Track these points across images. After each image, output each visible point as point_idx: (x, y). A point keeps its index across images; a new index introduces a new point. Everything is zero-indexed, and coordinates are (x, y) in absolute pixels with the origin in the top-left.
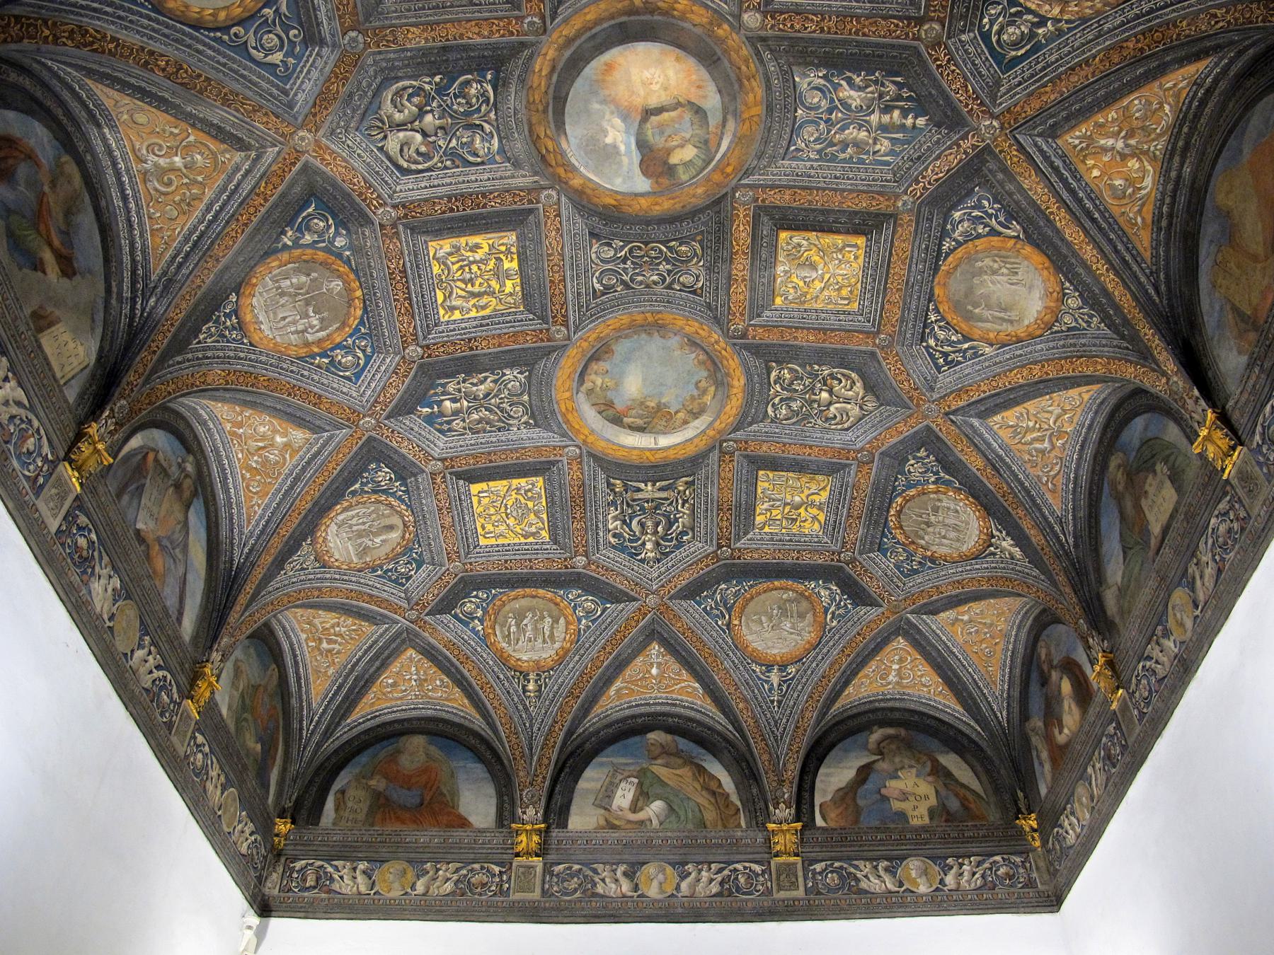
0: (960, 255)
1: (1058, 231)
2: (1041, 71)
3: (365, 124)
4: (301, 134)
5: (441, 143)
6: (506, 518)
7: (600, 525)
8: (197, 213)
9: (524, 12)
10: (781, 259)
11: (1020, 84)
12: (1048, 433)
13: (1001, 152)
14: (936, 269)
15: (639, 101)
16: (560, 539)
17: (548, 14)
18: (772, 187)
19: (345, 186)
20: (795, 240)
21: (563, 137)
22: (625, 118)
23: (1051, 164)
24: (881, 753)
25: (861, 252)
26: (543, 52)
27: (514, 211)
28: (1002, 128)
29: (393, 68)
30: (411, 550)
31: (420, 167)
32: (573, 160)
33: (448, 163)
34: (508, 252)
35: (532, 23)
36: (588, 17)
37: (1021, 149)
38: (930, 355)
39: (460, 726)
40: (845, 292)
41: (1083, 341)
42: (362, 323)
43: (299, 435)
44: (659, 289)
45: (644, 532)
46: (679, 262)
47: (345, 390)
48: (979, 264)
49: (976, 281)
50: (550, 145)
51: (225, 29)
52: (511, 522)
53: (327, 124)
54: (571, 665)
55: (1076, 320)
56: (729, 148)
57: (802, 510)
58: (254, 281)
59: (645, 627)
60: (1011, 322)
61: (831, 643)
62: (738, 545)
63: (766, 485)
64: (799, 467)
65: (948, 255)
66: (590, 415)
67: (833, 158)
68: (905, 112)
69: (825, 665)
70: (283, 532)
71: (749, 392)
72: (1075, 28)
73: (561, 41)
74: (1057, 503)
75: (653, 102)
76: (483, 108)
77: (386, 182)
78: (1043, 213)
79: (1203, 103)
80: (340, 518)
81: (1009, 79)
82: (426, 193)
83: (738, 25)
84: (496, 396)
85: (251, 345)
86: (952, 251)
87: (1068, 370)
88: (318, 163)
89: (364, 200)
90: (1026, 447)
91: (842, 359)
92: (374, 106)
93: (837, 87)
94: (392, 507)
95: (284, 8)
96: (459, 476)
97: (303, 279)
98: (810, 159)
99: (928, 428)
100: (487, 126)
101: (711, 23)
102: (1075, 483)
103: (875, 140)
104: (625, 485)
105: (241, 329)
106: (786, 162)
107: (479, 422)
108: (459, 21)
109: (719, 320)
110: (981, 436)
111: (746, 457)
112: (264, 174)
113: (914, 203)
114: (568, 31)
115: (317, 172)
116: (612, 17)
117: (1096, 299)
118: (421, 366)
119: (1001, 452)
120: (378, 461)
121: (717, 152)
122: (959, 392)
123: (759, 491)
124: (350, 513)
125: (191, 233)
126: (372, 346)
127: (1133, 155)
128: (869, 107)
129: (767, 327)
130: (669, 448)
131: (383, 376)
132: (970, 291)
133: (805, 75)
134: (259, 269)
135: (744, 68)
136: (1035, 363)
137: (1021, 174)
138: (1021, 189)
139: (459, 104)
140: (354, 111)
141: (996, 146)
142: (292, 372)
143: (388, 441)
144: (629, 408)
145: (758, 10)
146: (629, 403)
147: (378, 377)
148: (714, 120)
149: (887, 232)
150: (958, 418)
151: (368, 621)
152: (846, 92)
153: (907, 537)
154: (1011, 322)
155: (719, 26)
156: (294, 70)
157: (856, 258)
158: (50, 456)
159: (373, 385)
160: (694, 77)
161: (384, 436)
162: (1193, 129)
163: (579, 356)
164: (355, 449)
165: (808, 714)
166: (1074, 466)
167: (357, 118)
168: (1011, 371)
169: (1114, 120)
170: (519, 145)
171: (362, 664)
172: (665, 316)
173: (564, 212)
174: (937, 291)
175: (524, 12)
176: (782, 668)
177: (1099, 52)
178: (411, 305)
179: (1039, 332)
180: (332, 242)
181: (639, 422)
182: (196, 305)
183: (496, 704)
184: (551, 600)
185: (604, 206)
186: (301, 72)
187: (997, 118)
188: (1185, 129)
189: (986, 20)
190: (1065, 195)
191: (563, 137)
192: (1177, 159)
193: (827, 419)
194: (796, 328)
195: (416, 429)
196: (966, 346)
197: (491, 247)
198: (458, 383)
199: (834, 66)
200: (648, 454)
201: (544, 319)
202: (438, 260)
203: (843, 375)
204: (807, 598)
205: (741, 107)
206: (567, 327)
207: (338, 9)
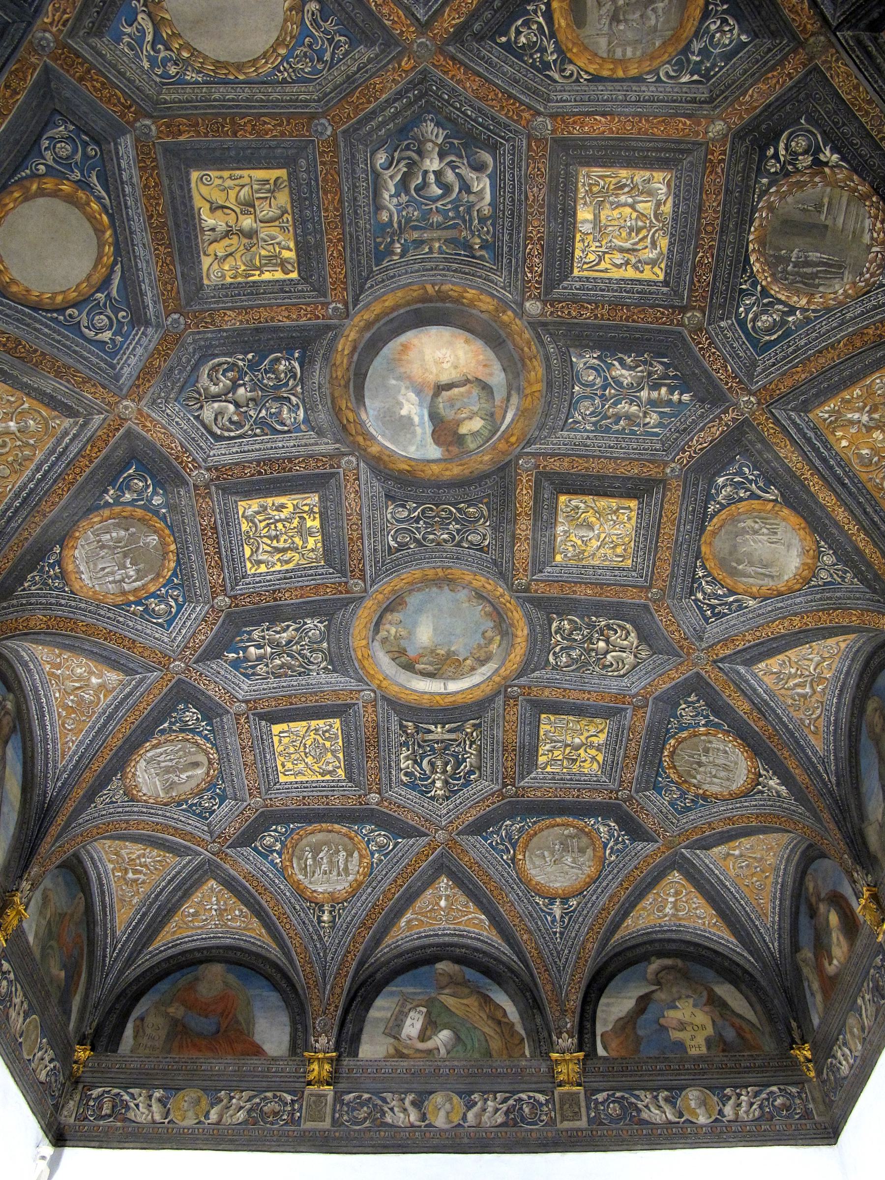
0: (724, 517)
1: (812, 495)
2: (792, 353)
3: (183, 395)
4: (125, 403)
5: (252, 413)
6: (305, 757)
7: (393, 764)
8: (28, 473)
9: (329, 299)
11: (774, 364)
12: (809, 679)
13: (758, 424)
14: (703, 529)
15: (431, 378)
16: (355, 776)
17: (350, 300)
18: (552, 455)
19: (164, 450)
20: (574, 503)
21: (363, 409)
22: (419, 392)
23: (804, 436)
24: (659, 983)
26: (346, 333)
27: (317, 475)
29: (208, 347)
30: (216, 785)
31: (232, 434)
32: (372, 430)
34: (311, 511)
35: (336, 309)
36: (387, 304)
37: (777, 422)
38: (699, 607)
39: (258, 956)
40: (619, 550)
42: (175, 574)
43: (113, 677)
44: (448, 546)
45: (433, 772)
46: (468, 523)
47: (157, 635)
48: (742, 525)
49: (739, 539)
50: (351, 416)
51: (61, 310)
52: (309, 760)
53: (149, 395)
54: (364, 898)
55: (831, 576)
56: (513, 420)
57: (581, 751)
58: (77, 534)
59: (434, 861)
60: (772, 577)
61: (610, 877)
62: (522, 784)
63: (548, 727)
64: (580, 711)
65: (713, 516)
66: (384, 660)
67: (608, 430)
69: (605, 899)
70: (94, 767)
71: (532, 639)
72: (821, 316)
73: (362, 324)
74: (818, 743)
75: (445, 378)
76: (290, 383)
77: (201, 447)
80: (149, 754)
81: (764, 360)
83: (521, 312)
84: (297, 643)
87: (826, 621)
88: (139, 429)
89: (181, 463)
90: (789, 693)
91: (617, 611)
92: (193, 379)
94: (198, 745)
95: (114, 293)
96: (262, 717)
97: (122, 533)
98: (586, 431)
99: (698, 674)
100: (293, 399)
101: (497, 310)
104: (416, 727)
105: (63, 578)
108: (271, 306)
109: (503, 575)
110: (747, 681)
111: (528, 701)
112: (91, 437)
113: (681, 470)
114: (368, 316)
115: (139, 437)
116: (408, 304)
117: (849, 557)
118: (229, 615)
119: (766, 697)
120: (186, 703)
121: (502, 423)
122: (726, 641)
123: (542, 733)
124: (158, 751)
125: (22, 489)
126: (184, 596)
127: (877, 428)
128: (639, 385)
129: (549, 582)
130: (457, 692)
131: (193, 623)
132: (734, 548)
133: (581, 356)
135: (526, 349)
136: (795, 614)
138: (777, 457)
139: (269, 379)
140: (174, 383)
141: (754, 419)
142: (108, 618)
143: (196, 683)
144: (421, 656)
145: (538, 298)
146: (421, 651)
148: (499, 396)
150: (726, 666)
151: (172, 852)
152: (618, 371)
153: (680, 777)
154: (772, 577)
155: (504, 312)
156: (121, 348)
157: (629, 519)
159: (184, 631)
160: (481, 357)
161: (193, 678)
164: (165, 690)
165: (589, 946)
166: (834, 709)
168: (773, 622)
169: (859, 397)
170: (322, 416)
171: (165, 894)
173: (363, 478)
174: (704, 549)
175: (329, 299)
176: (565, 900)
177: (843, 337)
178: (220, 558)
179: (798, 586)
180: (150, 501)
181: (430, 668)
182: (23, 556)
183: (292, 934)
184: (345, 835)
186: (127, 348)
187: (754, 394)
189: (741, 309)
190: (817, 463)
191: (363, 409)
193: (604, 667)
195: (222, 672)
196: (731, 599)
197: (296, 507)
198: (263, 631)
199: (607, 349)
200: (438, 698)
202: (246, 518)
203: (619, 626)
204: (587, 834)
205: (523, 384)
206: (364, 581)
207: (163, 295)
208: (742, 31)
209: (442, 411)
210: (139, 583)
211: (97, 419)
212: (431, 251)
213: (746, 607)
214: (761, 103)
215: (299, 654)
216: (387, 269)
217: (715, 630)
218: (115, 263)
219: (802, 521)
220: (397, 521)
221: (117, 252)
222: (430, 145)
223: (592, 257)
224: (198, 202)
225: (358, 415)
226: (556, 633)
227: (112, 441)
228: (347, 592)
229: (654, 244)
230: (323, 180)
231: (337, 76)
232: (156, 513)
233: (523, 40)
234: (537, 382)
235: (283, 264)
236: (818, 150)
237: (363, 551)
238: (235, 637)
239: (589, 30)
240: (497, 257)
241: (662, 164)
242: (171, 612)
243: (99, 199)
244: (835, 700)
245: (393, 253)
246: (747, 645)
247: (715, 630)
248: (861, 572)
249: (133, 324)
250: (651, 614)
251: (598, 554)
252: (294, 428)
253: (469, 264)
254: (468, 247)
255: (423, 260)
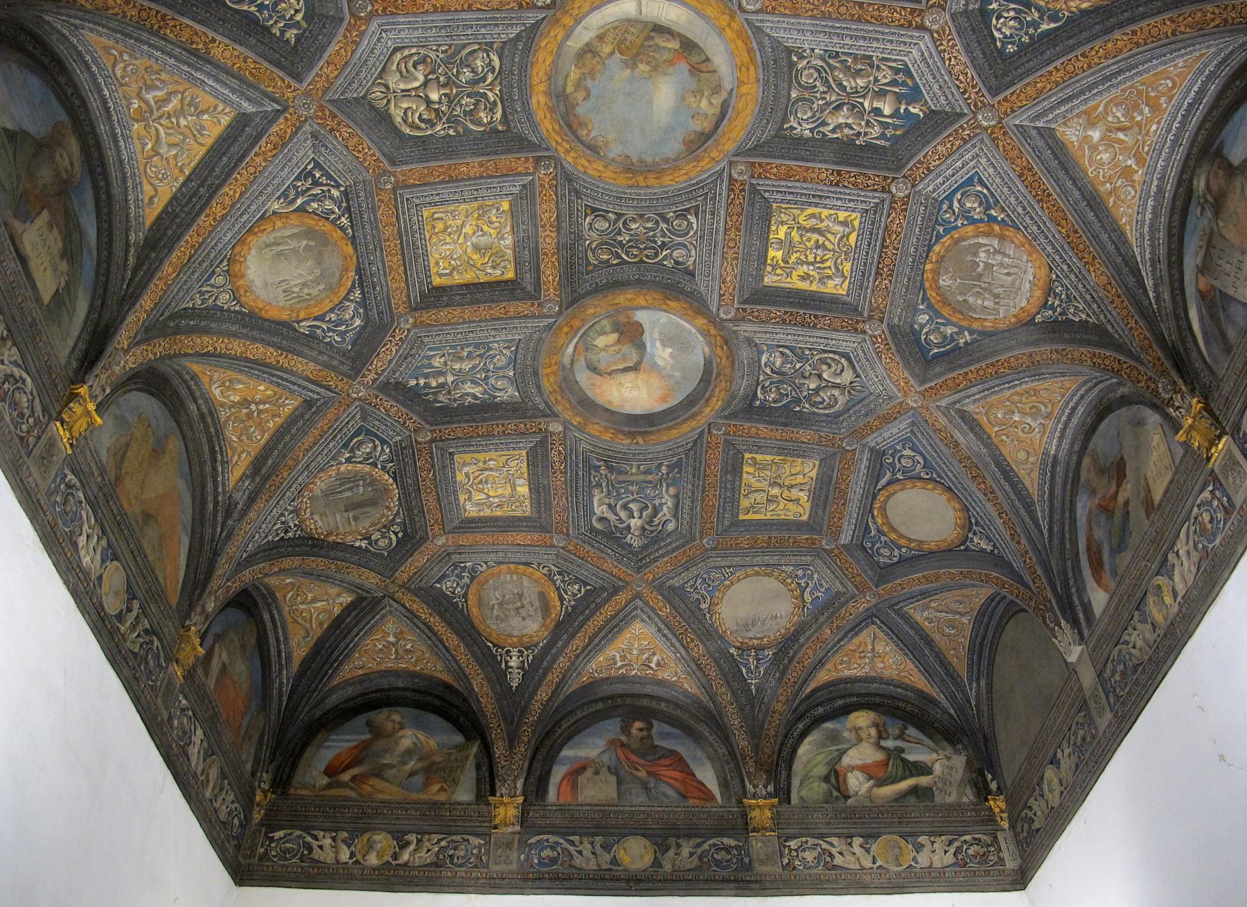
3: (863, 395)
8: (1024, 386)
10: (510, 252)
12: (156, 114)
14: (359, 270)
15: (642, 376)
18: (526, 316)
20: (498, 272)
22: (654, 367)
25: (434, 270)
28: (348, 395)
29: (831, 422)
31: (831, 355)
32: (701, 338)
33: (807, 352)
34: (774, 267)
37: (328, 388)
38: (330, 177)
40: (440, 226)
41: (197, 274)
42: (939, 237)
43: (1070, 134)
44: (631, 214)
46: (609, 243)
47: (991, 170)
48: (321, 287)
50: (719, 351)
51: (931, 479)
55: (213, 286)
60: (268, 246)
65: (353, 286)
67: (477, 346)
68: (427, 385)
70: (1168, 28)
75: (630, 376)
78: (288, 351)
79: (213, 451)
82: (835, 335)
83: (567, 425)
84: (828, 104)
85: (1051, 269)
86: (350, 291)
88: (912, 382)
90: (171, 88)
91: (425, 148)
92: (851, 403)
93: (485, 392)
95: (888, 474)
97: (971, 300)
98: (497, 342)
99: (298, 78)
100: (768, 371)
102: (86, 63)
103: (446, 364)
105: (1050, 289)
106: (517, 337)
107: (858, 73)
110: (233, 90)
113: (399, 324)
118: (898, 170)
119: (198, 75)
120: (1001, 52)
126: (940, 209)
129: (513, 174)
131: (947, 168)
134: (1002, 326)
136: (224, 217)
137: (320, 371)
138: (315, 361)
140: (868, 405)
142: (1032, 219)
144: (671, 63)
145: (552, 434)
146: (671, 70)
147: (950, 172)
148: (581, 363)
149: (415, 295)
150: (270, 107)
152: (477, 391)
154: (268, 246)
157: (437, 263)
158: (1211, 488)
159: (959, 164)
162: (207, 432)
163: (723, 141)
166: (100, 80)
167: (867, 401)
168: (242, 194)
172: (625, 182)
173: (716, 297)
174: (350, 250)
178: (884, 240)
179: (238, 249)
181: (660, 41)
185: (678, 300)
188: (212, 430)
192: (205, 410)
193: (423, 61)
194: (481, 177)
195: (936, 87)
196: (299, 201)
197: (789, 275)
199: (489, 405)
201: (754, 190)
202: (843, 275)
203: (419, 128)
208: (441, 589)
209: (634, 351)
210: (981, 241)
211: (943, 403)
212: (638, 467)
213: (279, 198)
214: (416, 556)
215: (830, 87)
216: (674, 456)
217: (302, 153)
218: (880, 490)
219: (266, 316)
220: (686, 246)
221: (874, 497)
222: (637, 533)
223: (513, 464)
224: (808, 506)
225: (711, 350)
226: (495, 103)
227: (940, 381)
228: (753, 164)
229: (467, 475)
230: (713, 512)
231: (694, 571)
232: (930, 306)
233: (576, 587)
234: (548, 375)
235: (755, 463)
236: (370, 544)
237: (728, 214)
238: (903, 136)
239: (537, 590)
240: (586, 461)
241: (472, 521)
242: (962, 195)
243: (875, 523)
244: (106, 92)
245: (668, 466)
246: (256, 149)
247: (302, 153)
248: (191, 317)
249: (884, 453)
250: (384, 155)
251: (462, 217)
252: (772, 345)
253: (609, 457)
254: (610, 468)
255: (645, 460)
